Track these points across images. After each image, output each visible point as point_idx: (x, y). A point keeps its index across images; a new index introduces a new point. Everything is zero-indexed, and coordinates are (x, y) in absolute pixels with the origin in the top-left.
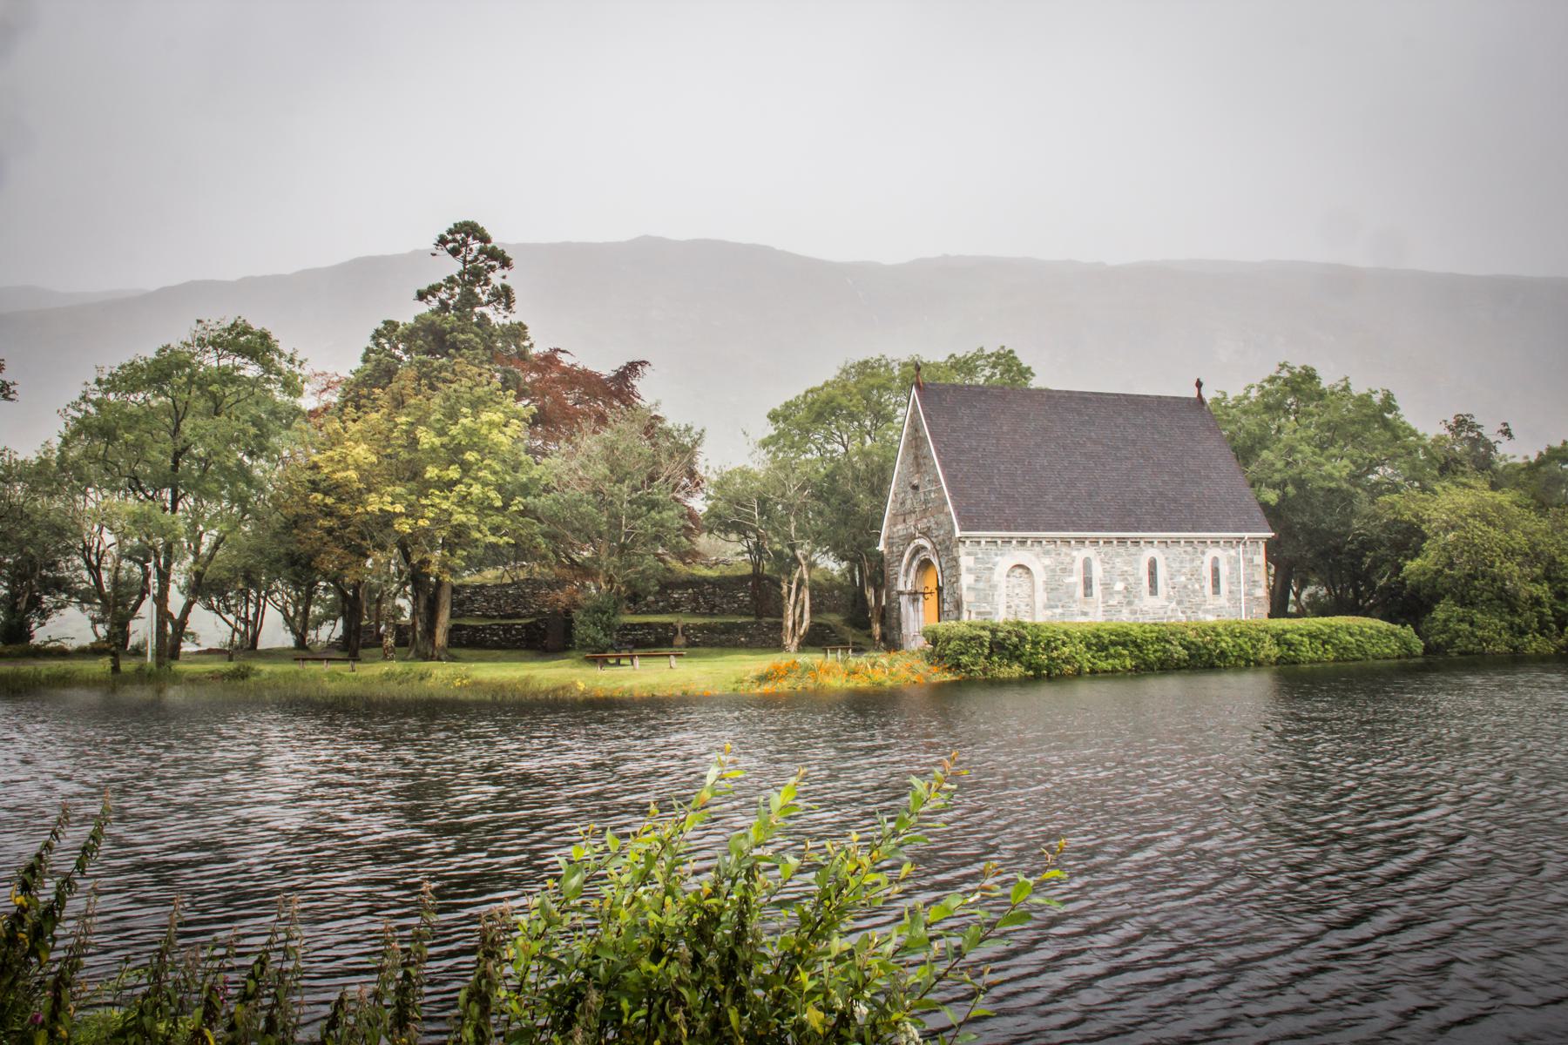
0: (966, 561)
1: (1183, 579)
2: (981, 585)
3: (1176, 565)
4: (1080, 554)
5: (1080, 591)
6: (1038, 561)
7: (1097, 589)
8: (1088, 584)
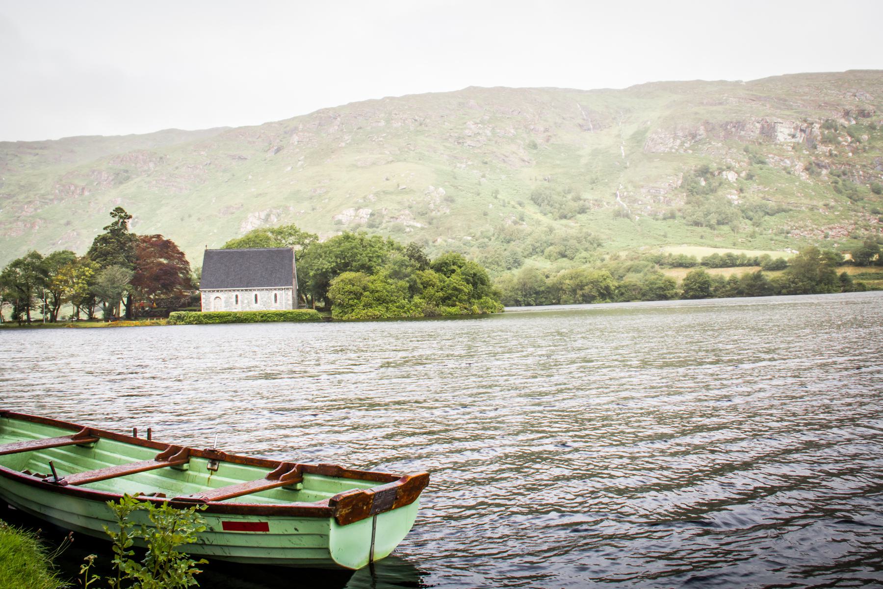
4: (234, 294)
5: (235, 302)
6: (223, 295)
7: (239, 302)
8: (237, 301)
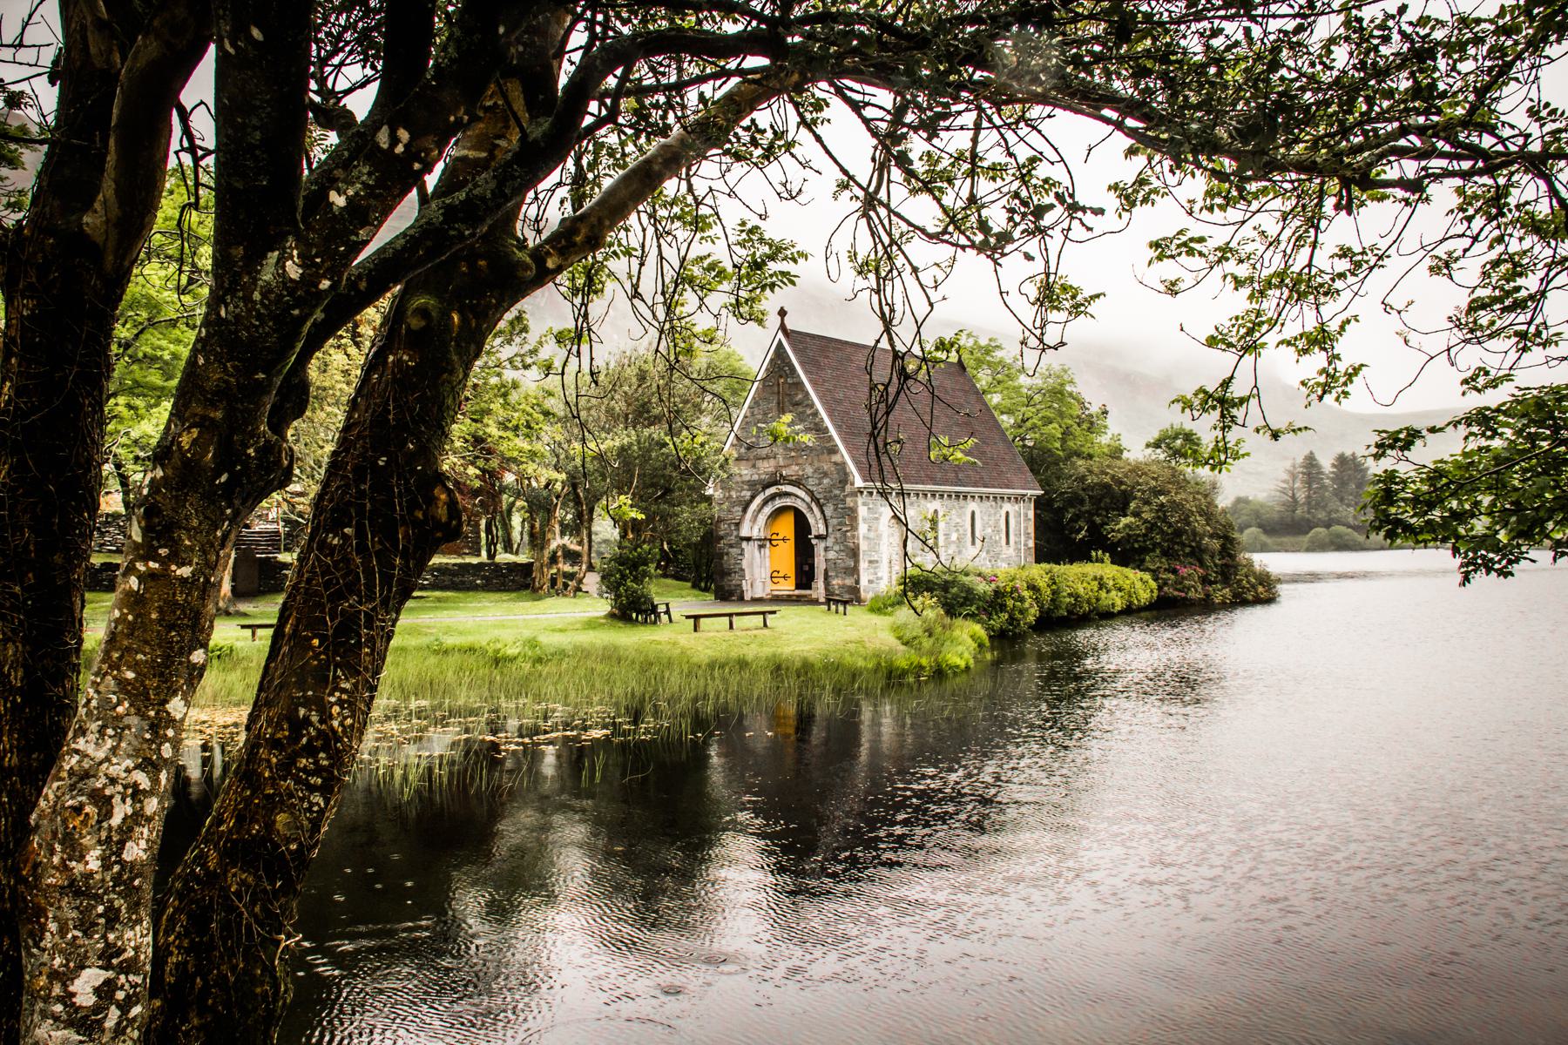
0: (862, 511)
1: (989, 530)
2: (872, 535)
3: (986, 518)
